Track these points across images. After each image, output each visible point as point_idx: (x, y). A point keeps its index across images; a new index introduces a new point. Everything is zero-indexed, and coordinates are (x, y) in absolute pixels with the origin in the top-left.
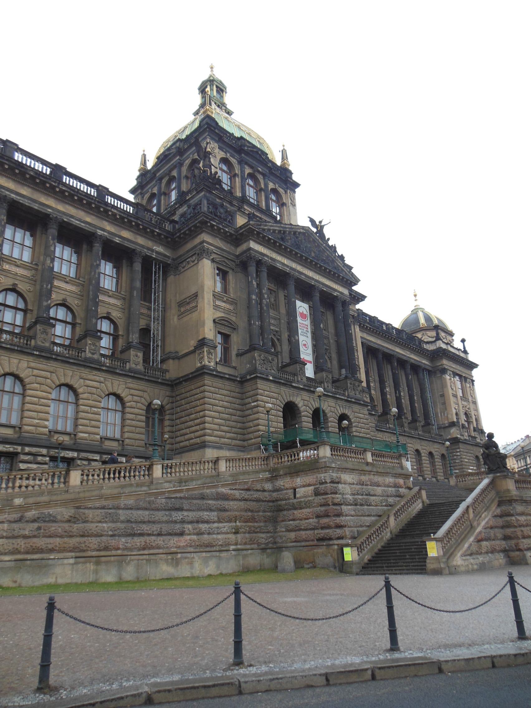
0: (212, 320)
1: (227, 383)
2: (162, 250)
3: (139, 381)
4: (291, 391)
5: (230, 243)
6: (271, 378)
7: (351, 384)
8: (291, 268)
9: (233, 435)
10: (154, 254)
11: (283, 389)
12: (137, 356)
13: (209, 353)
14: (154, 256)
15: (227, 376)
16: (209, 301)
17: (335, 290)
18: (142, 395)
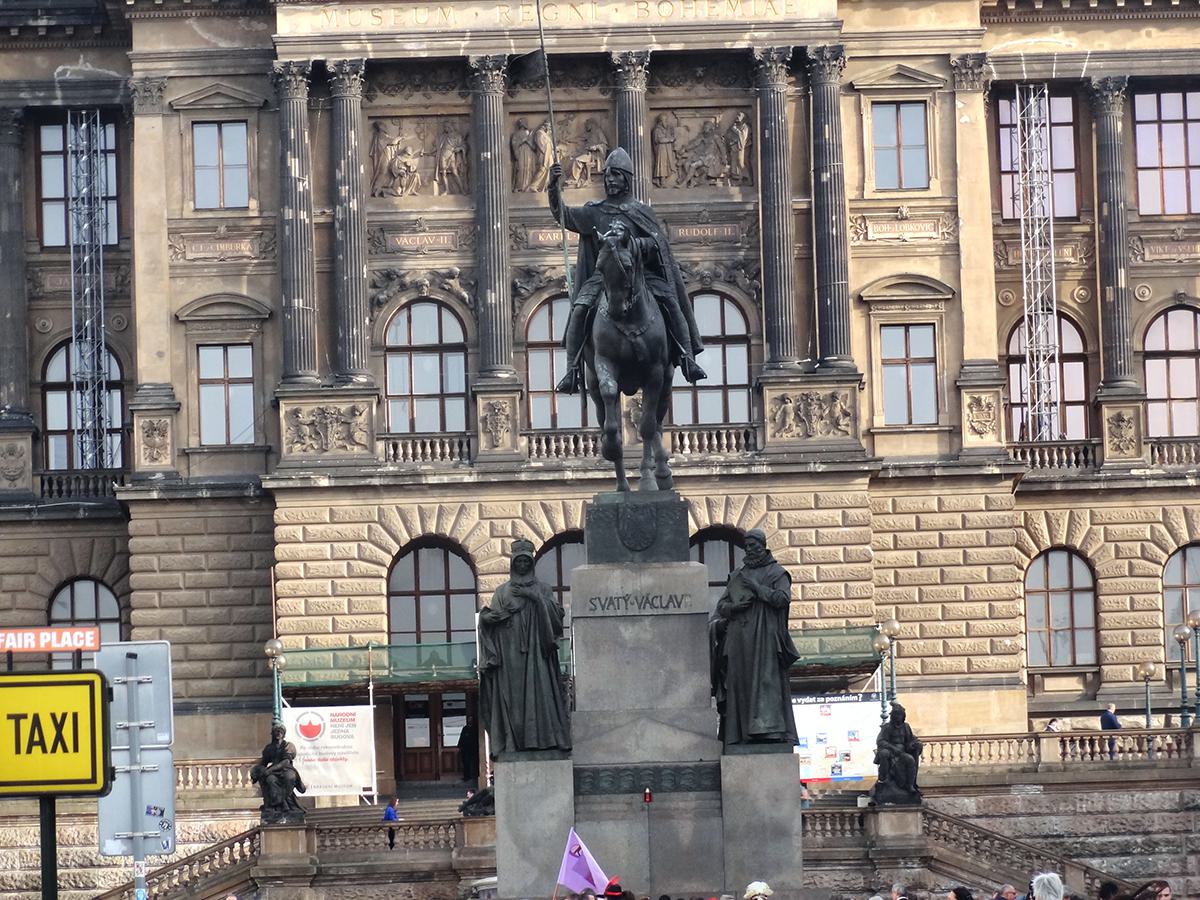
0: (164, 317)
1: (215, 511)
2: (89, 67)
3: (19, 530)
4: (431, 502)
5: (244, 15)
6: (324, 482)
7: (783, 400)
8: (477, 34)
9: (232, 665)
10: (59, 93)
11: (390, 503)
12: (12, 452)
13: (151, 431)
14: (58, 102)
15: (205, 494)
16: (154, 261)
17: (742, 28)
18: (31, 567)
